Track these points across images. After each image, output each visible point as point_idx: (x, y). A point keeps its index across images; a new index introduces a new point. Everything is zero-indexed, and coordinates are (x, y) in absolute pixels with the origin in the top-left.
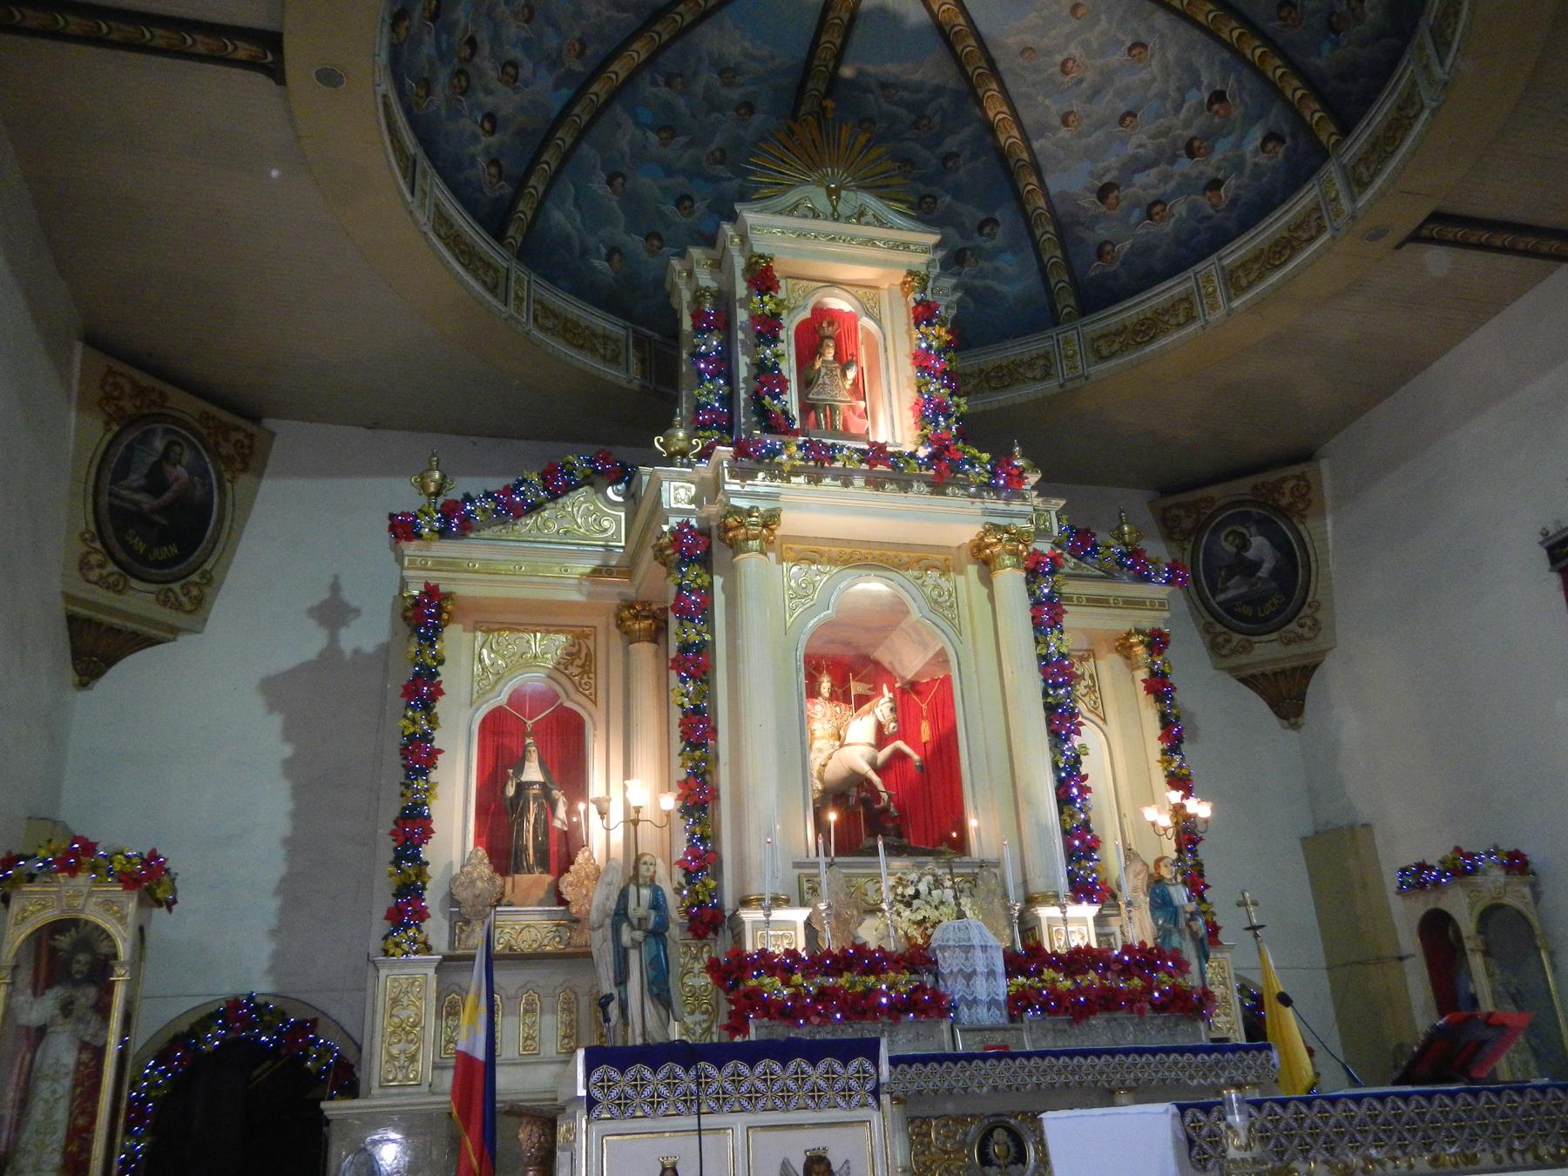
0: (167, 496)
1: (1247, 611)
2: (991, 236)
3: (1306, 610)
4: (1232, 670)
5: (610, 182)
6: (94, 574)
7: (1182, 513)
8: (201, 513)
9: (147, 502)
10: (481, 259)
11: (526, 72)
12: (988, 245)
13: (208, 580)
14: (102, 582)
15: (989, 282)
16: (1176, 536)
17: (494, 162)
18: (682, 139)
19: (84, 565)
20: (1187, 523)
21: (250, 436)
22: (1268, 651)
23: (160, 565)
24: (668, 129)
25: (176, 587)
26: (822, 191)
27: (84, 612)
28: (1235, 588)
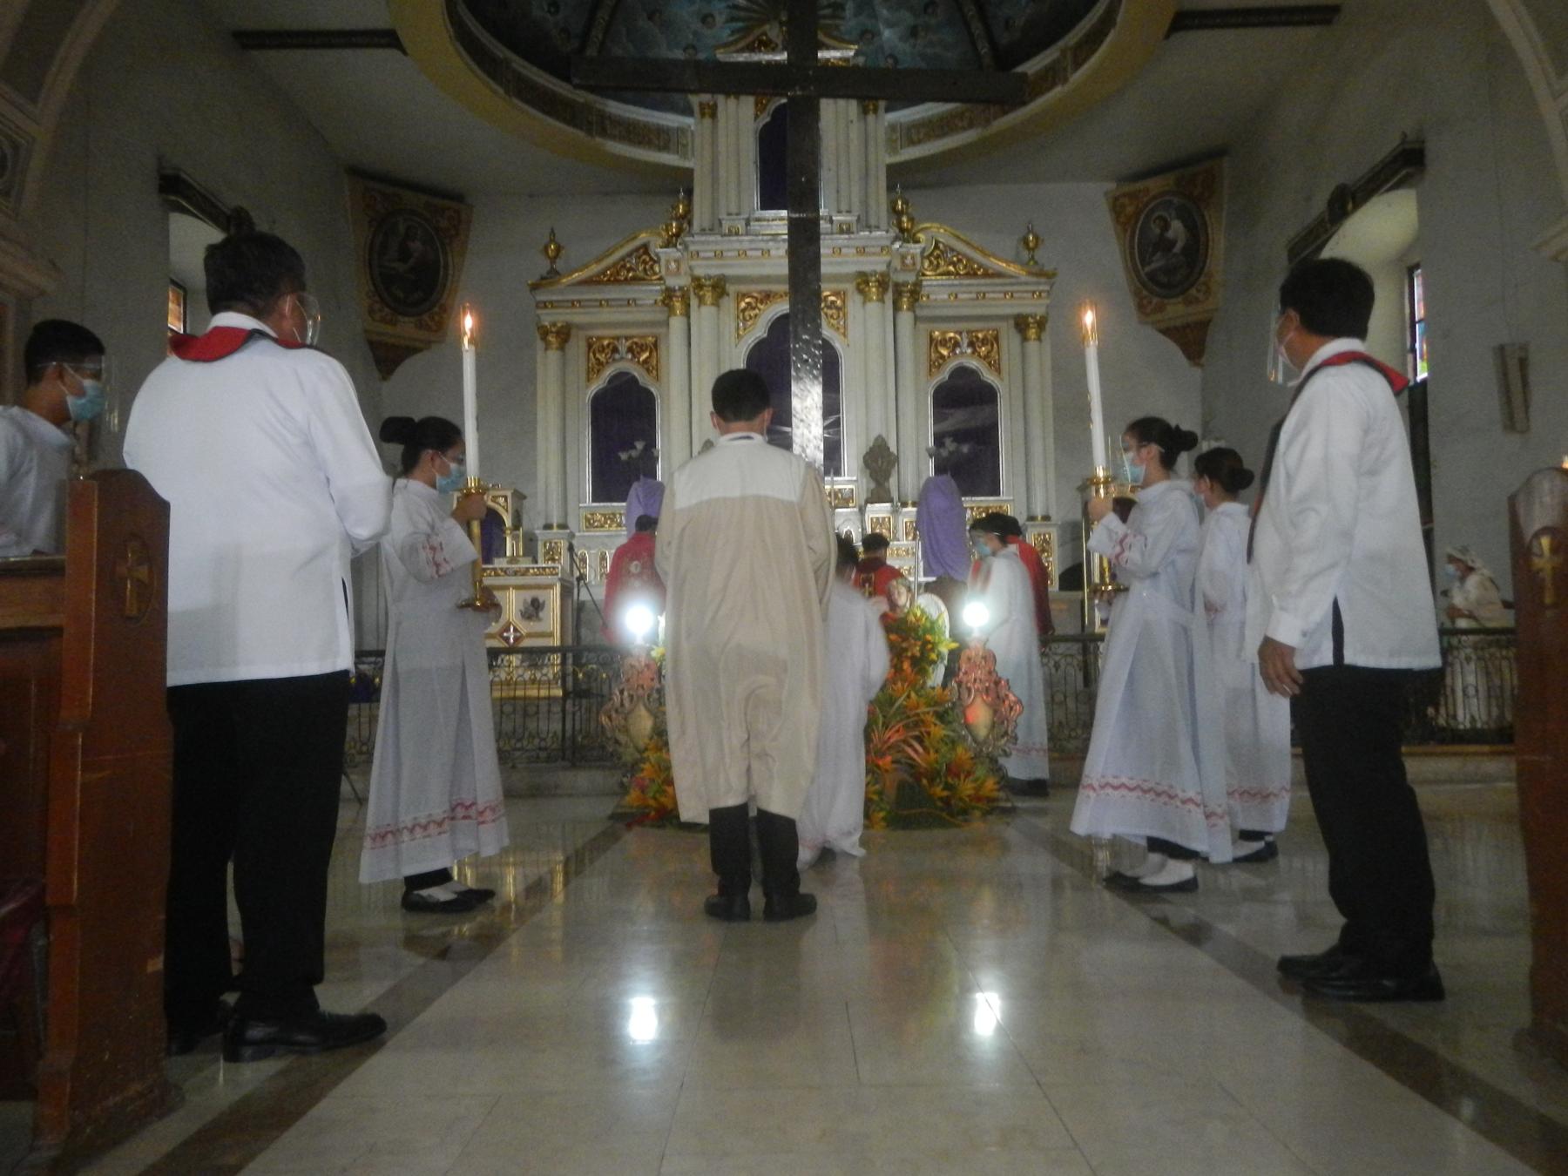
0: (412, 261)
1: (1164, 279)
3: (1202, 279)
4: (1153, 323)
5: (650, 18)
6: (377, 316)
7: (1126, 201)
13: (444, 309)
14: (383, 320)
16: (1122, 219)
19: (371, 312)
20: (1130, 209)
22: (1176, 310)
25: (425, 317)
26: (776, 25)
28: (1158, 262)
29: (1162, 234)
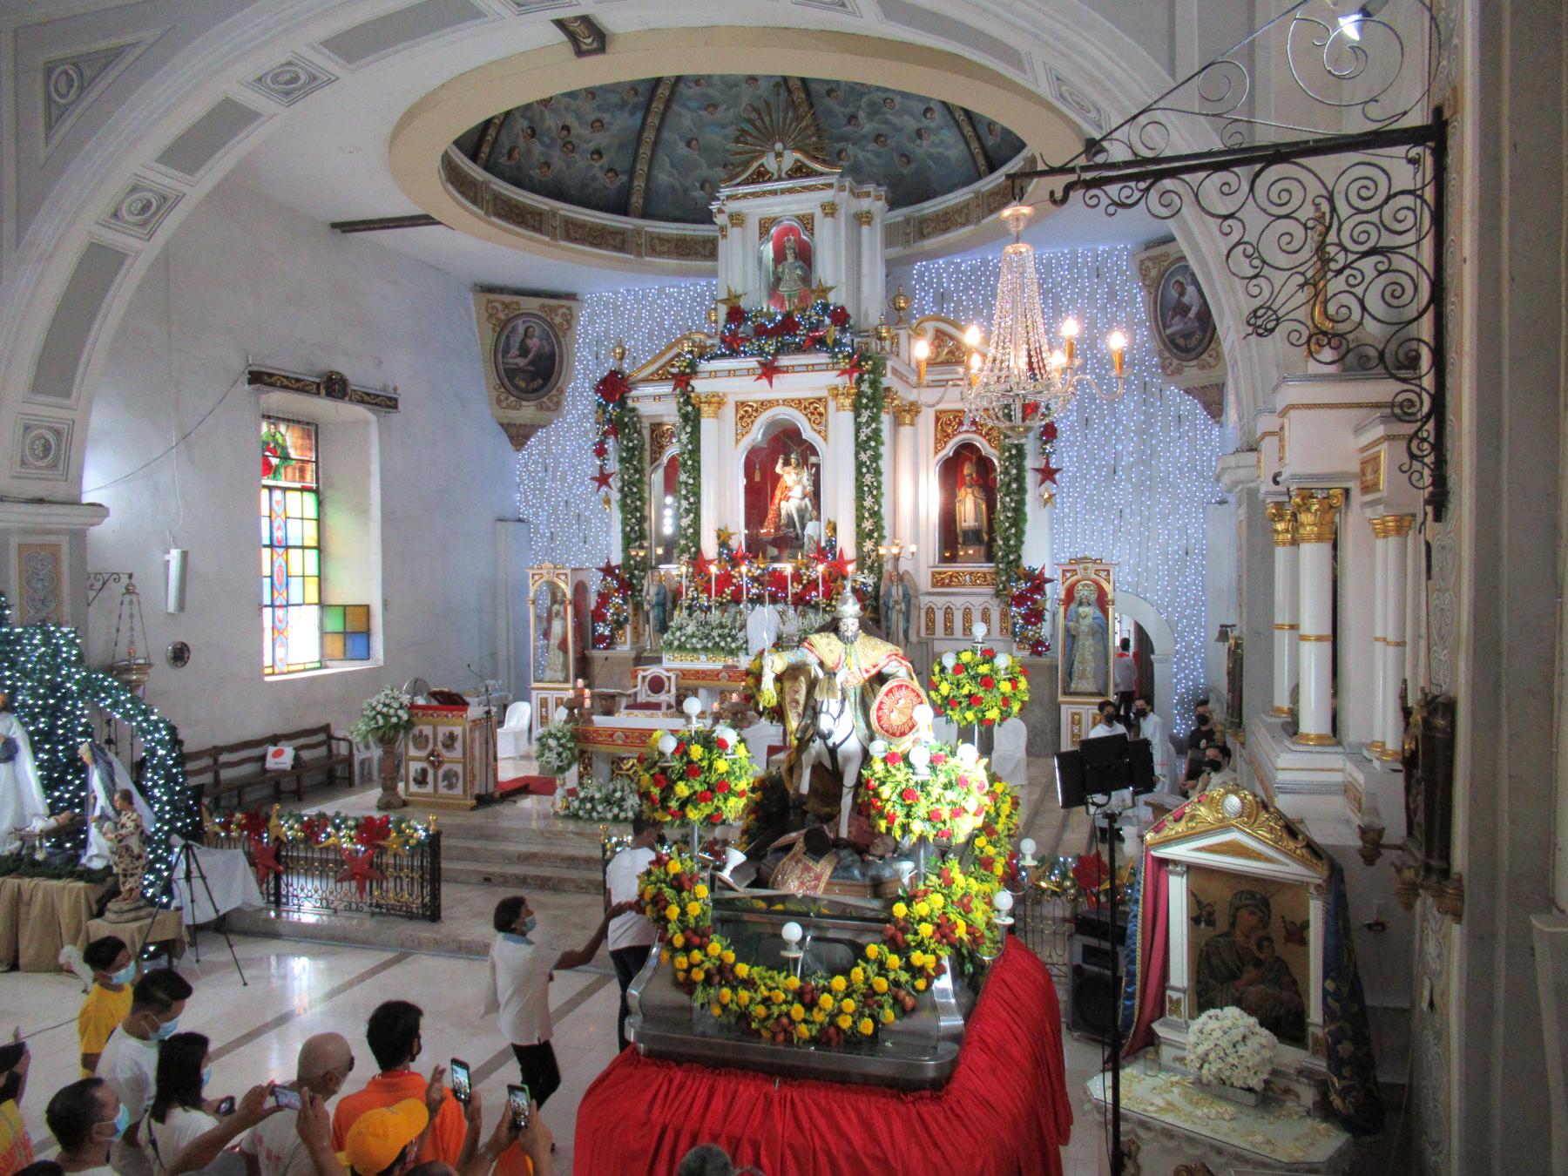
0: (531, 356)
1: (1181, 342)
2: (932, 119)
3: (1213, 345)
5: (688, 145)
8: (551, 358)
9: (522, 362)
10: (611, 233)
11: (606, 117)
12: (933, 125)
13: (561, 392)
14: (509, 407)
15: (940, 150)
17: (610, 170)
18: (723, 107)
19: (499, 401)
20: (1154, 273)
21: (569, 308)
22: (1193, 373)
23: (535, 391)
24: (712, 106)
26: (771, 156)
27: (505, 421)
28: (1176, 326)
29: (1179, 301)
